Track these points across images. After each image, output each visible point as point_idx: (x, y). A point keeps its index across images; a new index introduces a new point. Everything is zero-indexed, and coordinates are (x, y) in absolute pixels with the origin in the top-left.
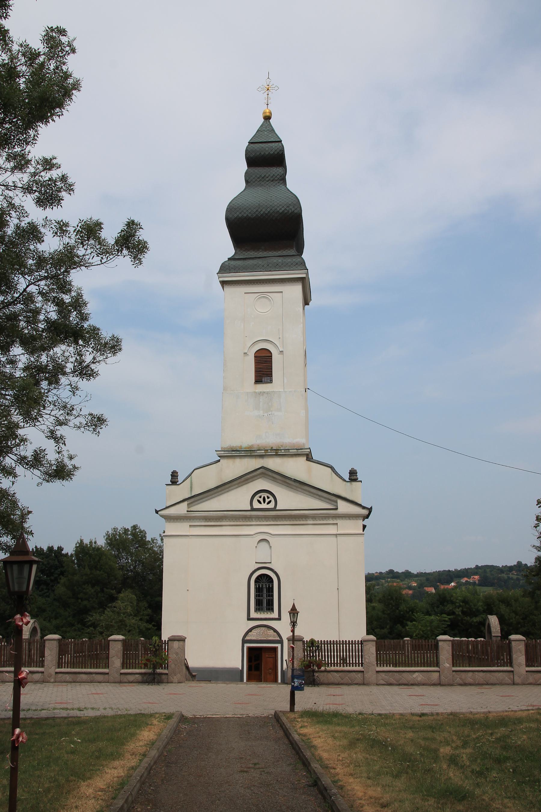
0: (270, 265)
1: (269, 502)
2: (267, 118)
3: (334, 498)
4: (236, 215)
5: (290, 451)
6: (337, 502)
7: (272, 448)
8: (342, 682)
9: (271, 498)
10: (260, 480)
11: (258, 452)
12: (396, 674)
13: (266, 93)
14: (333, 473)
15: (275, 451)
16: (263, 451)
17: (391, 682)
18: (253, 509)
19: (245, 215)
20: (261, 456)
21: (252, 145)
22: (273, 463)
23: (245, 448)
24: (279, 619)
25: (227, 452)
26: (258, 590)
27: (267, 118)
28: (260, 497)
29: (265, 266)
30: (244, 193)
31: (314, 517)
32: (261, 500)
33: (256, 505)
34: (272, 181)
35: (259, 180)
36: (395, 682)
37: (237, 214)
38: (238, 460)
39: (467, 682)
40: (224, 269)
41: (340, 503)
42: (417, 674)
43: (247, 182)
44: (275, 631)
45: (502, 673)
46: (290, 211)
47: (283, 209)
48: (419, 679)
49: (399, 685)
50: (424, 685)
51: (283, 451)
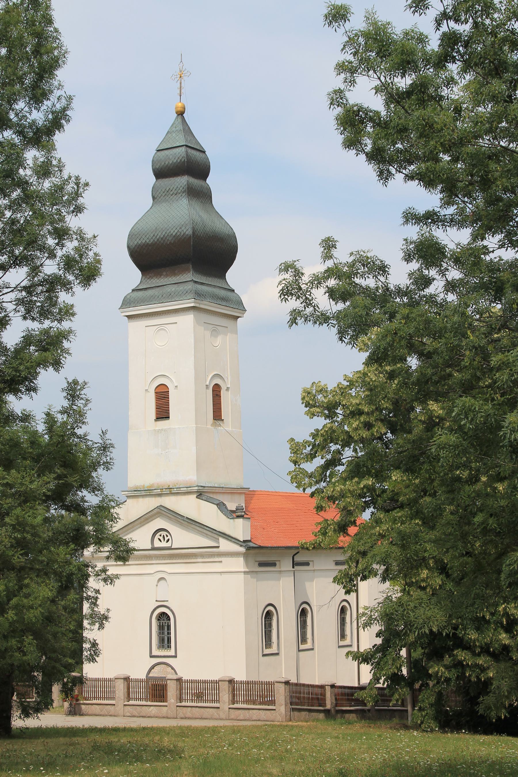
0: (164, 296)
1: (168, 540)
2: (181, 114)
3: (216, 536)
4: (136, 243)
5: (181, 489)
6: (219, 540)
7: (169, 486)
8: (101, 713)
9: (169, 537)
10: (158, 518)
11: (155, 491)
12: (137, 707)
13: (179, 82)
14: (219, 510)
15: (168, 490)
16: (159, 491)
17: (134, 714)
18: (153, 549)
19: (144, 242)
20: (160, 495)
21: (159, 153)
22: (169, 502)
23: (147, 487)
24: (175, 657)
25: (130, 493)
26: (161, 628)
27: (181, 114)
28: (161, 536)
29: (160, 296)
30: (151, 210)
31: (202, 556)
32: (161, 538)
33: (157, 544)
34: (176, 194)
35: (164, 194)
36: (137, 715)
37: (136, 242)
38: (141, 500)
39: (187, 716)
40: (127, 303)
41: (221, 540)
42: (152, 707)
43: (154, 198)
44: (173, 668)
45: (212, 709)
46: (182, 234)
47: (176, 231)
48: (153, 712)
49: (140, 717)
50: (156, 717)
51: (175, 489)
